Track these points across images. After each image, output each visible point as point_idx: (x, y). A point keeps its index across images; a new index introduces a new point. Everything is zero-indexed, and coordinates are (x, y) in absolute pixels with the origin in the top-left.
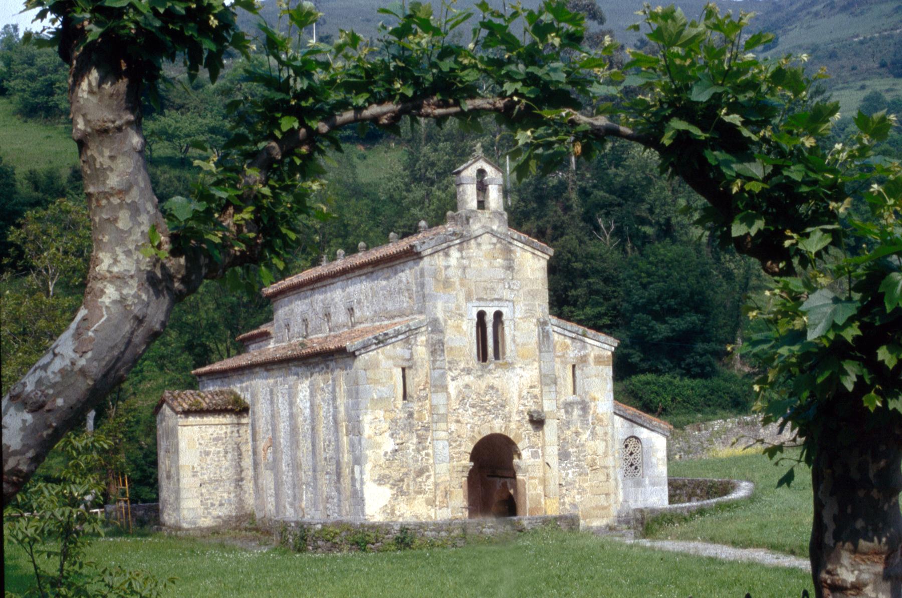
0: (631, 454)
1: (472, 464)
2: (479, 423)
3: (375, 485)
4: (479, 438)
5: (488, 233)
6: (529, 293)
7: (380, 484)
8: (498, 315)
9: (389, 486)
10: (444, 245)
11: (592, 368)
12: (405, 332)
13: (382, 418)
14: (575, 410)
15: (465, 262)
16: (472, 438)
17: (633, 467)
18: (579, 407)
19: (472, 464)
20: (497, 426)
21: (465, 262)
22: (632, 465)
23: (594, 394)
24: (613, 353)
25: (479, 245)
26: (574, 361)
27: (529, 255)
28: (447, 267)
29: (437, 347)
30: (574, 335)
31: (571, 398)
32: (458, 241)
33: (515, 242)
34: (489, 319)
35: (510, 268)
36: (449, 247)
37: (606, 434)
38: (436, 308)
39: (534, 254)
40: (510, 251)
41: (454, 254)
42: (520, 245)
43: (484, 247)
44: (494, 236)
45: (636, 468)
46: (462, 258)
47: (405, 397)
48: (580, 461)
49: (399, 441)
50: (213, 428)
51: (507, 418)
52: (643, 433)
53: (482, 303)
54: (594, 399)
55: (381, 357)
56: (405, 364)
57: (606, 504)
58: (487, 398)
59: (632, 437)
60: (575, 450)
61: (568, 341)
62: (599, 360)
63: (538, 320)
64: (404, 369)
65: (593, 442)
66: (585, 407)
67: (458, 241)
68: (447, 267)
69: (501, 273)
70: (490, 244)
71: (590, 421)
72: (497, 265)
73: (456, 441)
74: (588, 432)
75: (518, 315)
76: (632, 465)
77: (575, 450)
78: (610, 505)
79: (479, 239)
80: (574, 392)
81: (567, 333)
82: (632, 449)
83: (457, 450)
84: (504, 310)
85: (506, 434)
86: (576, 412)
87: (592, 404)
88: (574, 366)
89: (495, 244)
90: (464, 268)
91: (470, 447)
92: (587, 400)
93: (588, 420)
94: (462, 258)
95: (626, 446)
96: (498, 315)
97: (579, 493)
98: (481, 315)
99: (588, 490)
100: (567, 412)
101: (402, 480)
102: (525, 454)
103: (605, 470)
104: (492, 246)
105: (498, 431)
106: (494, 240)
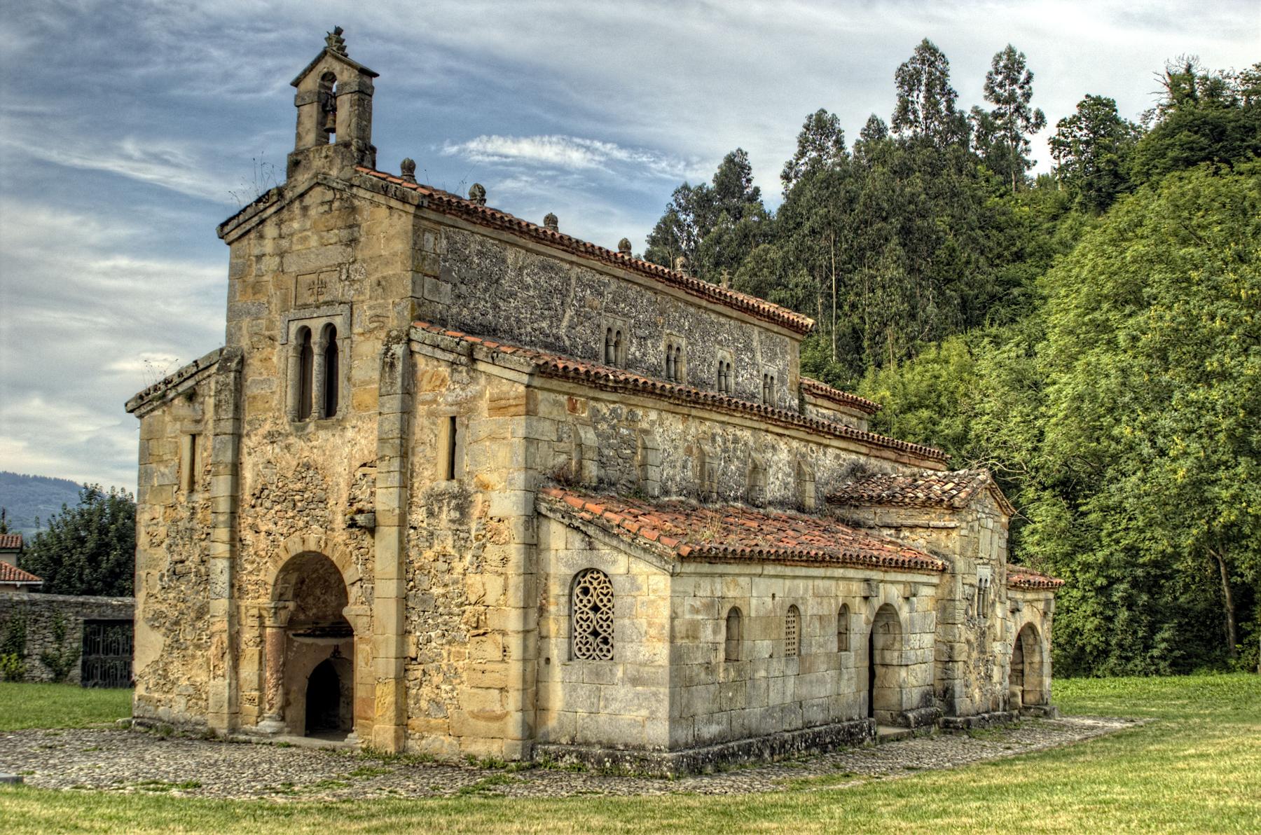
2: (285, 531)
3: (147, 628)
4: (286, 557)
5: (318, 184)
6: (379, 284)
7: (153, 627)
8: (330, 330)
9: (163, 630)
10: (256, 219)
11: (483, 422)
12: (192, 375)
13: (161, 519)
14: (445, 509)
15: (285, 243)
16: (275, 558)
17: (599, 640)
18: (454, 502)
20: (313, 539)
21: (285, 243)
23: (486, 477)
25: (305, 209)
27: (384, 211)
28: (259, 258)
29: (222, 397)
30: (451, 357)
31: (443, 485)
32: (273, 209)
33: (361, 193)
34: (316, 338)
35: (352, 242)
36: (262, 222)
37: (505, 561)
38: (240, 329)
39: (390, 208)
40: (353, 210)
41: (270, 230)
42: (368, 195)
43: (313, 212)
44: (330, 188)
45: (605, 641)
46: (281, 237)
48: (450, 614)
49: (176, 557)
51: (327, 526)
52: (618, 564)
53: (302, 314)
54: (485, 487)
55: (167, 418)
56: (194, 429)
57: (498, 709)
58: (299, 486)
59: (592, 570)
60: (441, 591)
61: (444, 370)
62: (499, 407)
63: (388, 336)
64: (194, 437)
65: (478, 577)
66: (462, 503)
67: (273, 209)
68: (259, 258)
69: (336, 254)
70: (323, 203)
71: (473, 533)
72: (332, 241)
73: (253, 562)
74: (468, 557)
75: (357, 329)
77: (441, 591)
78: (507, 714)
79: (308, 200)
80: (451, 476)
81: (439, 354)
83: (254, 578)
84: (338, 322)
85: (328, 552)
86: (447, 515)
87: (479, 498)
88: (453, 419)
89: (331, 202)
90: (282, 254)
91: (270, 573)
92: (471, 489)
93: (469, 532)
94: (281, 237)
96: (330, 330)
97: (447, 680)
98: (306, 333)
99: (465, 676)
100: (431, 514)
101: (177, 623)
102: (354, 592)
103: (499, 638)
104: (326, 207)
105: (312, 546)
106: (329, 195)
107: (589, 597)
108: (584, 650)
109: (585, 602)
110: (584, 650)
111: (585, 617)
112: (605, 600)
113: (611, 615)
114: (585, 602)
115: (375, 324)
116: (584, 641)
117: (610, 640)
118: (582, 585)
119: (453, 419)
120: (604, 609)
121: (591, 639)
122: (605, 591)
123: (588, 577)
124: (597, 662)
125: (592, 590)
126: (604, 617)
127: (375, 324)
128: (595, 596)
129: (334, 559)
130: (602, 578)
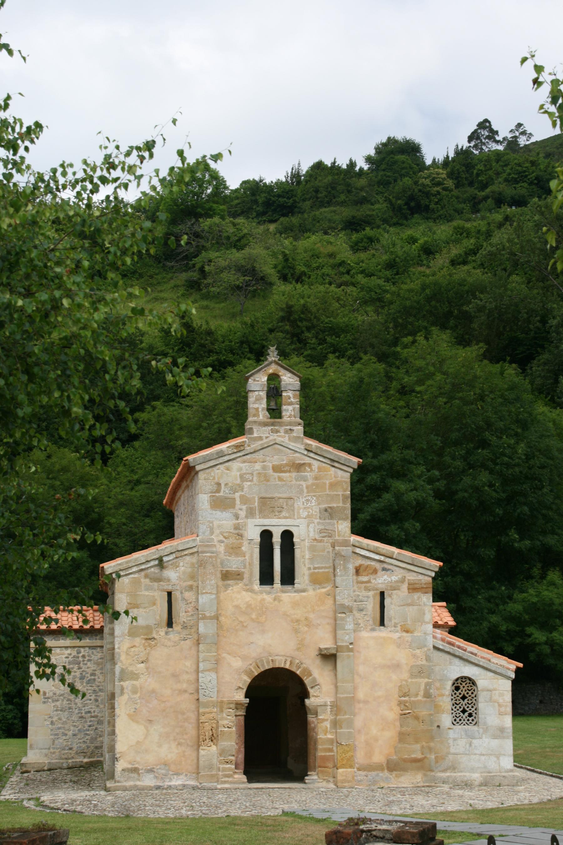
0: (464, 698)
1: (247, 700)
16: (248, 672)
17: (466, 714)
19: (247, 700)
22: (464, 711)
24: (434, 579)
26: (382, 587)
34: (277, 539)
45: (470, 715)
47: (170, 624)
50: (69, 651)
62: (413, 588)
76: (464, 711)
82: (464, 692)
88: (382, 594)
95: (457, 688)
96: (287, 536)
98: (266, 535)
107: (460, 691)
108: (458, 720)
109: (458, 694)
110: (458, 720)
111: (458, 702)
112: (470, 693)
113: (474, 702)
114: (458, 694)
115: (325, 534)
116: (458, 715)
117: (474, 714)
118: (456, 685)
119: (382, 594)
120: (470, 698)
121: (462, 714)
122: (470, 688)
123: (459, 681)
124: (466, 726)
125: (461, 687)
126: (470, 702)
127: (325, 534)
128: (464, 690)
129: (298, 672)
130: (468, 681)
